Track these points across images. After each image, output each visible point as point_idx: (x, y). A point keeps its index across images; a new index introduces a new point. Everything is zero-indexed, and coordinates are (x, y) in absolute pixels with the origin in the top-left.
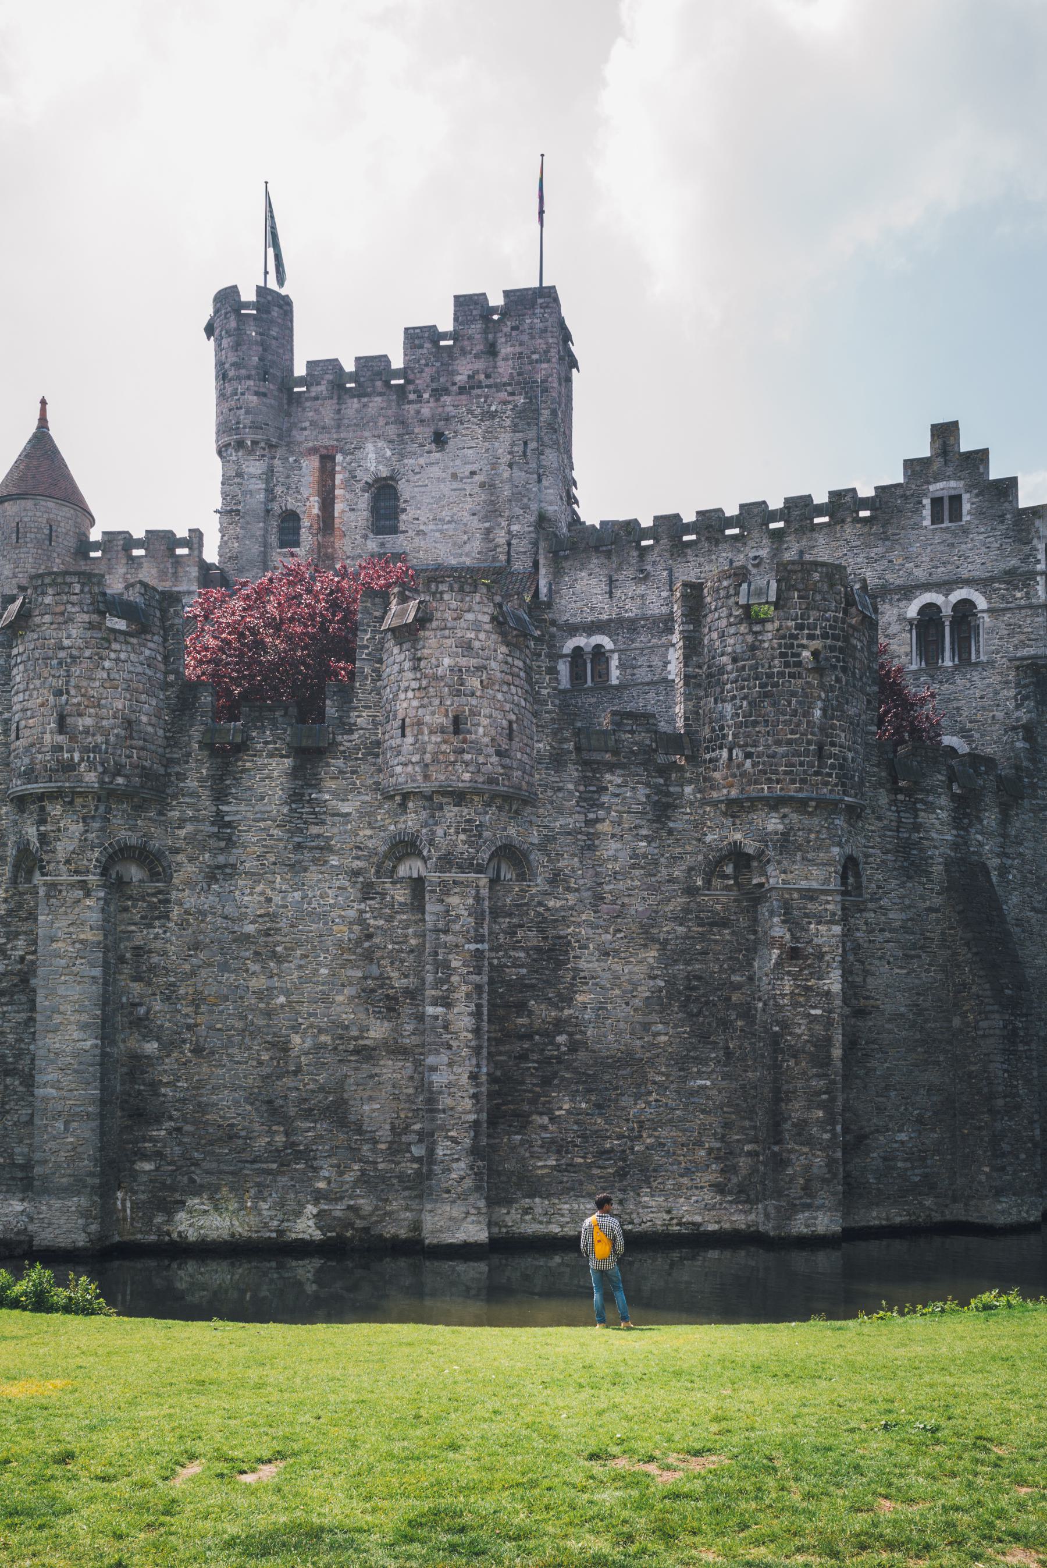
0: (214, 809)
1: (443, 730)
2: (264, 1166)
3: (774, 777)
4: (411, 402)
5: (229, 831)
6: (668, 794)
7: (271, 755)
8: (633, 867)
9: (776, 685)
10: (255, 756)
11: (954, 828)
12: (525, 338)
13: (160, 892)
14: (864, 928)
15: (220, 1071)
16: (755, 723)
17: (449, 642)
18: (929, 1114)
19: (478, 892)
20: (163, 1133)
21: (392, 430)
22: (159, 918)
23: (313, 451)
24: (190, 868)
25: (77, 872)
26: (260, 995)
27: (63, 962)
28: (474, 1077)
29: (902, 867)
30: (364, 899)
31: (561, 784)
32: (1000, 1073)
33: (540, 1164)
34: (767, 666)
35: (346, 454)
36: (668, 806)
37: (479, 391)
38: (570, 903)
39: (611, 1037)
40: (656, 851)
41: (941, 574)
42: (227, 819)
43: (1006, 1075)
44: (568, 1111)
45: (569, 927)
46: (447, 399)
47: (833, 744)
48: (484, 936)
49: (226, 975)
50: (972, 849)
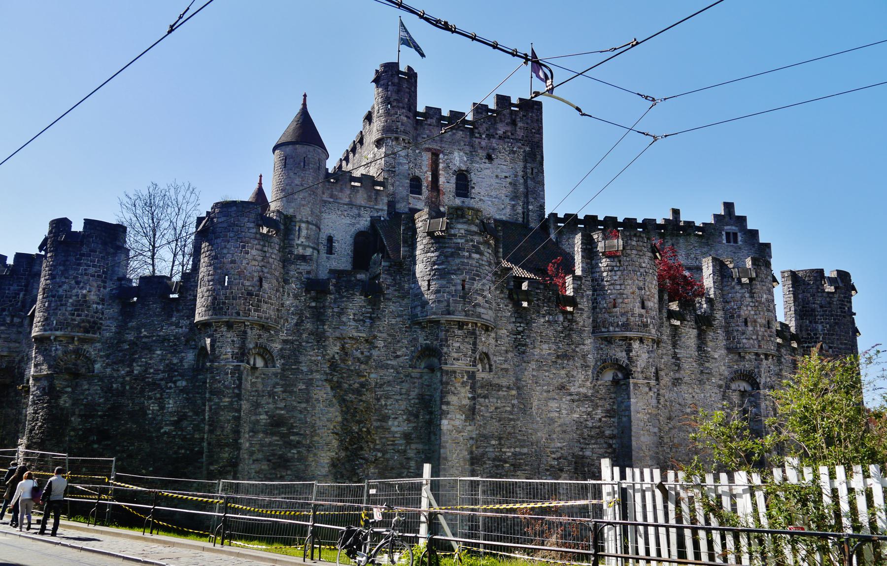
7: (690, 327)
9: (839, 320)
16: (833, 335)
21: (467, 149)
23: (428, 150)
35: (444, 155)
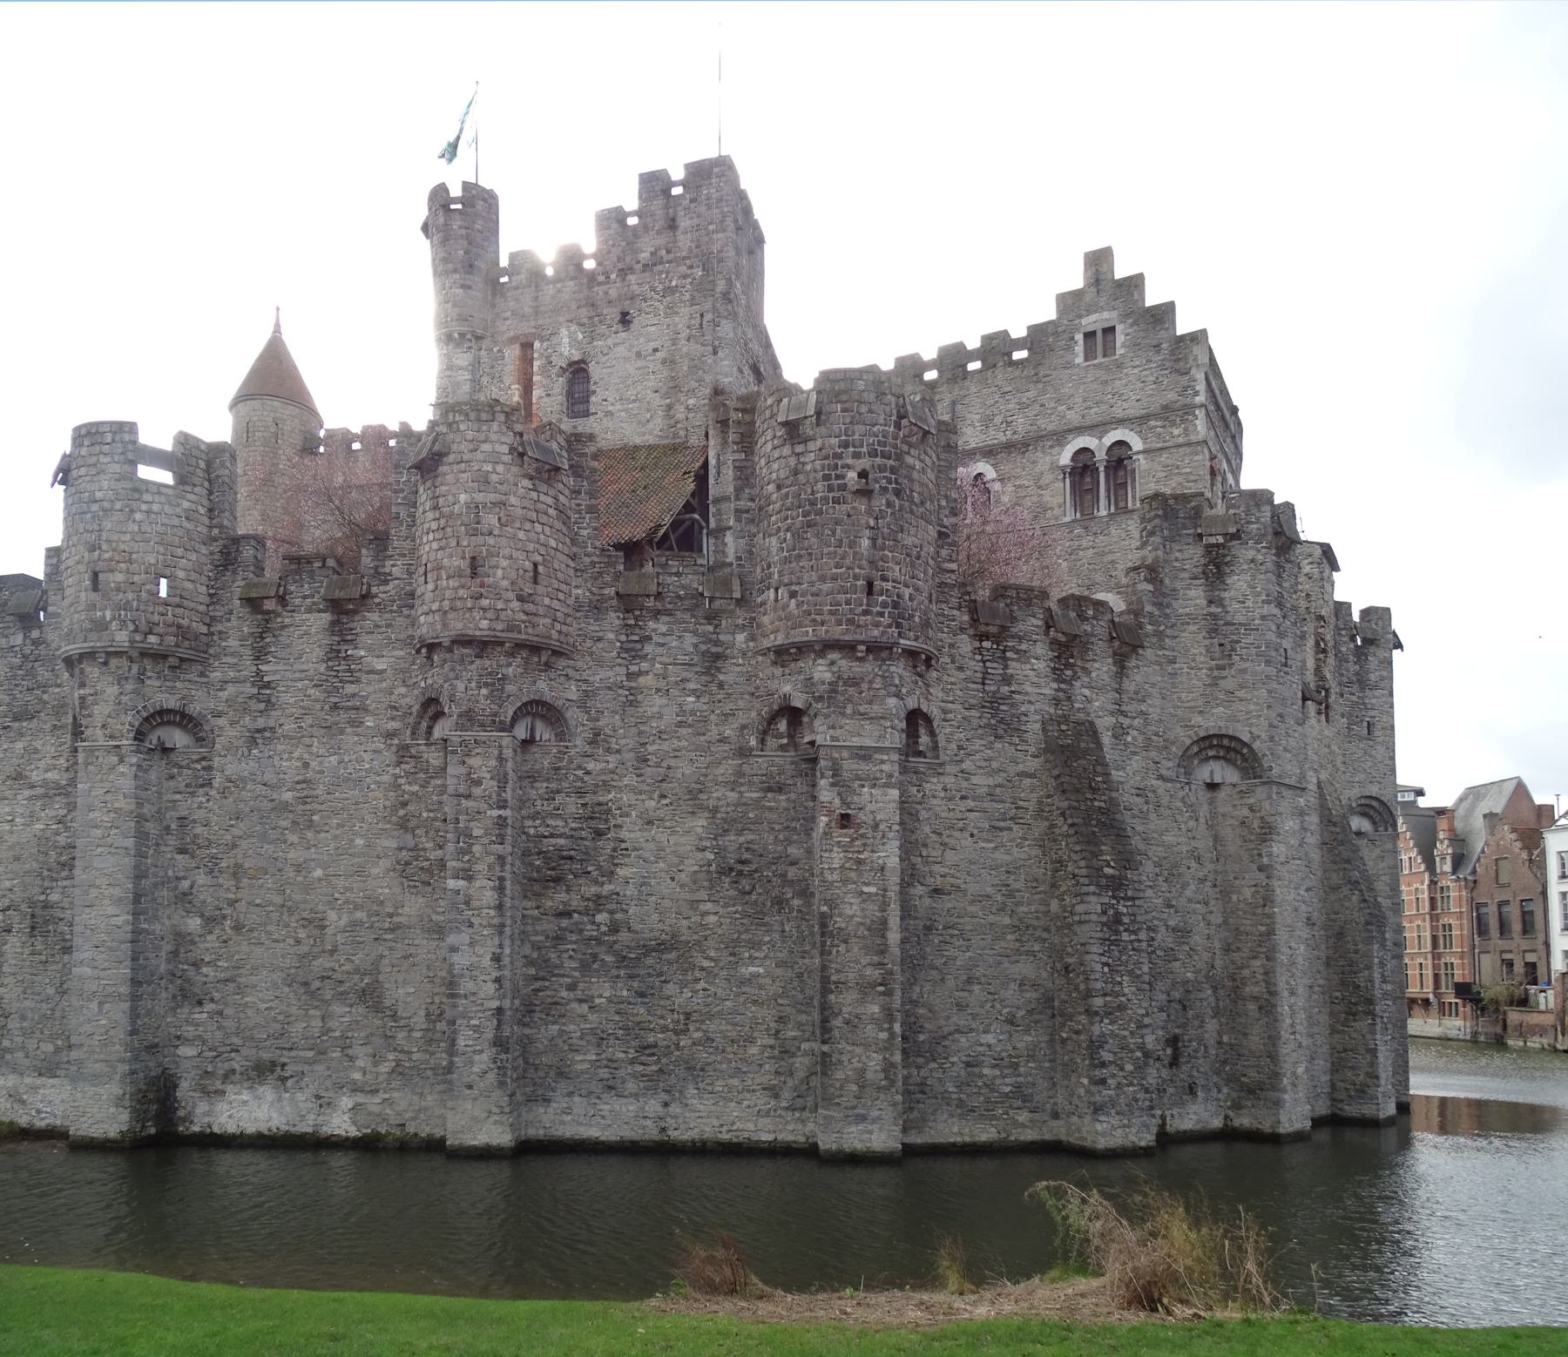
0: (255, 668)
1: (459, 574)
2: (302, 1053)
3: (818, 618)
4: (599, 284)
5: (268, 692)
6: (717, 643)
7: (309, 611)
8: (680, 724)
9: (820, 513)
10: (294, 611)
11: (1055, 680)
12: (703, 209)
13: (204, 759)
15: (258, 950)
17: (464, 476)
19: (501, 753)
20: (205, 1015)
22: (202, 786)
23: (513, 340)
24: (231, 732)
25: (112, 737)
26: (298, 868)
27: (99, 832)
28: (497, 959)
30: (399, 763)
31: (601, 634)
33: (579, 1058)
34: (809, 491)
36: (718, 657)
37: (660, 267)
38: (611, 766)
39: (655, 917)
40: (705, 707)
42: (266, 679)
44: (610, 1000)
45: (609, 792)
46: (632, 278)
47: (884, 579)
48: (506, 801)
49: (266, 846)
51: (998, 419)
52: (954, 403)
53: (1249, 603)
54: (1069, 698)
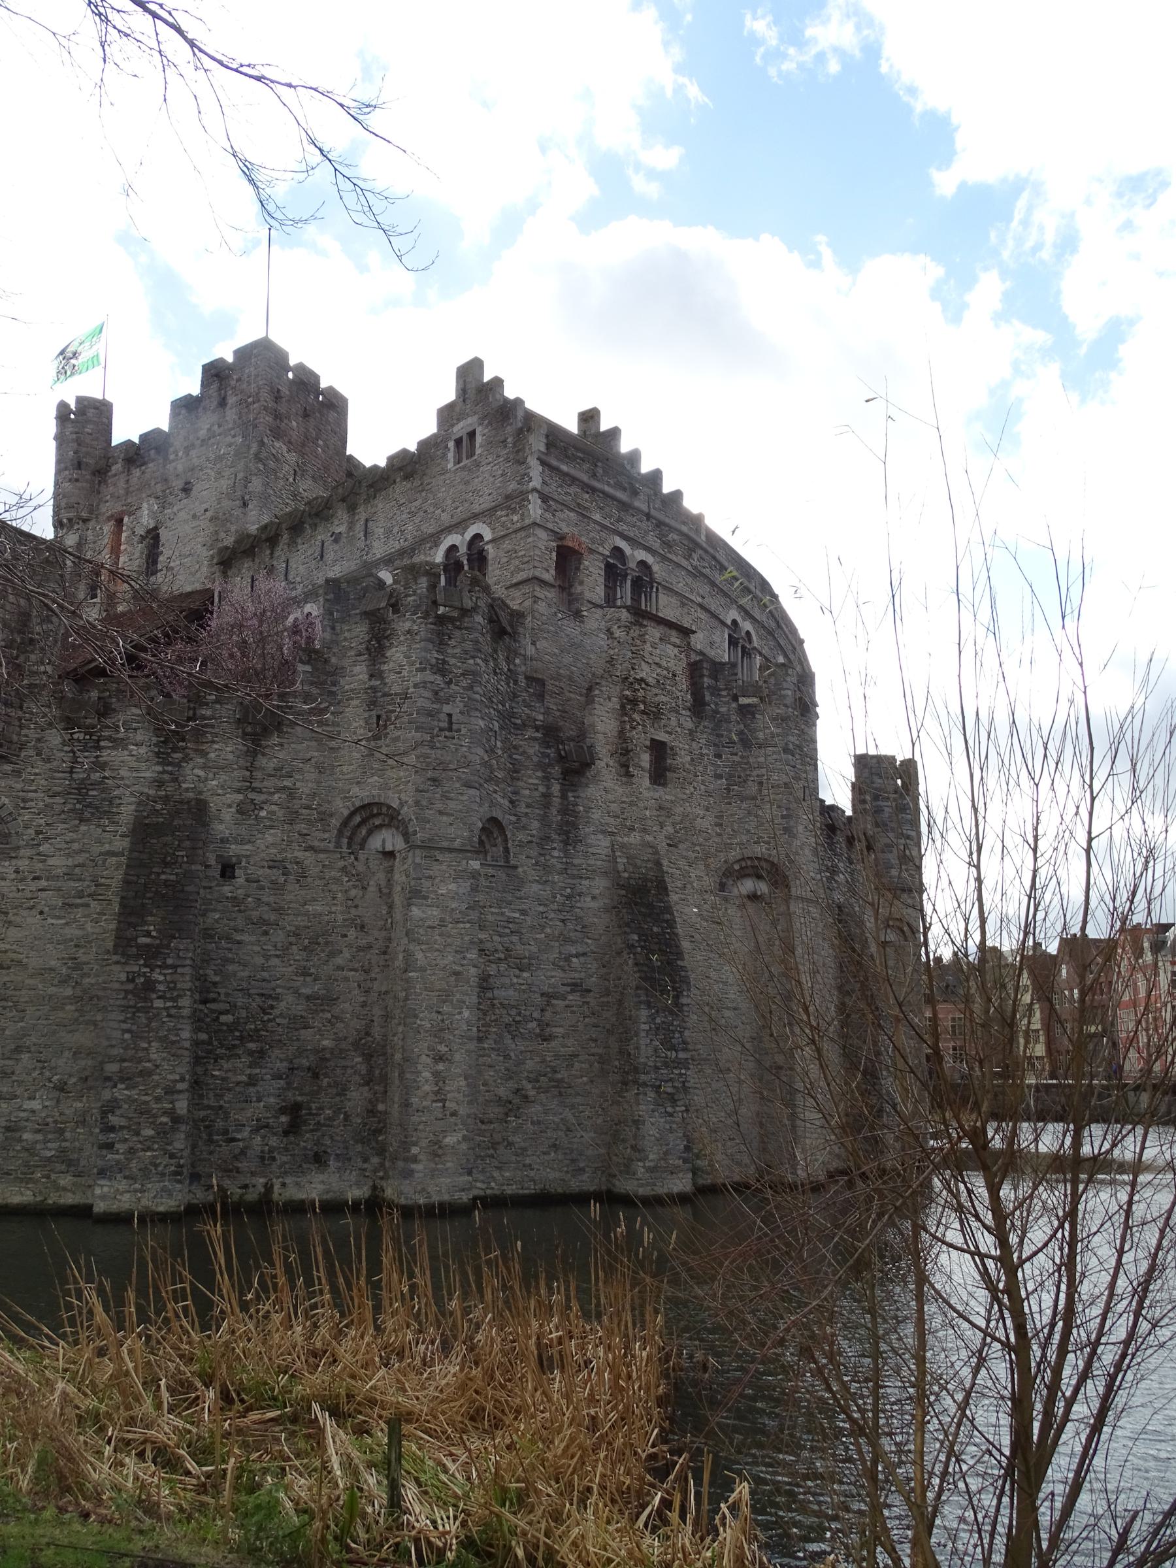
11: (158, 764)
14: (13, 876)
18: (73, 1080)
29: (73, 810)
32: (117, 1034)
41: (461, 513)
43: (127, 1036)
50: (184, 786)
51: (396, 529)
52: (367, 520)
53: (405, 673)
54: (176, 780)
